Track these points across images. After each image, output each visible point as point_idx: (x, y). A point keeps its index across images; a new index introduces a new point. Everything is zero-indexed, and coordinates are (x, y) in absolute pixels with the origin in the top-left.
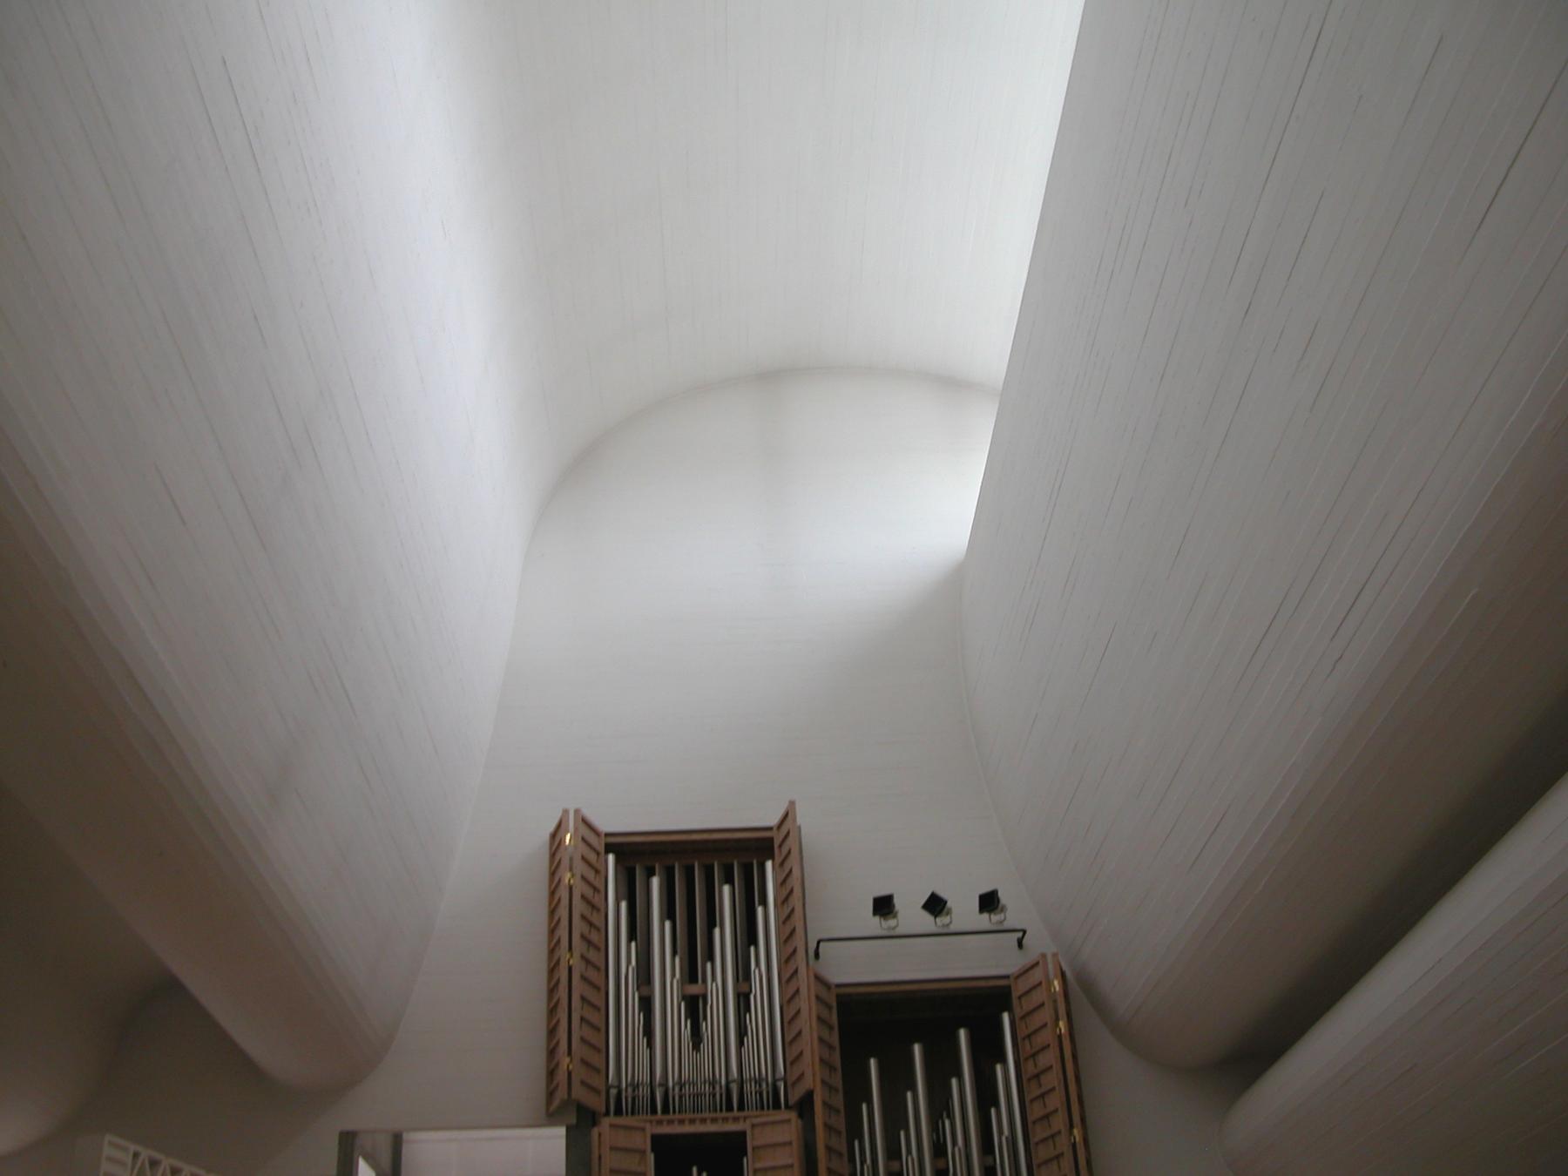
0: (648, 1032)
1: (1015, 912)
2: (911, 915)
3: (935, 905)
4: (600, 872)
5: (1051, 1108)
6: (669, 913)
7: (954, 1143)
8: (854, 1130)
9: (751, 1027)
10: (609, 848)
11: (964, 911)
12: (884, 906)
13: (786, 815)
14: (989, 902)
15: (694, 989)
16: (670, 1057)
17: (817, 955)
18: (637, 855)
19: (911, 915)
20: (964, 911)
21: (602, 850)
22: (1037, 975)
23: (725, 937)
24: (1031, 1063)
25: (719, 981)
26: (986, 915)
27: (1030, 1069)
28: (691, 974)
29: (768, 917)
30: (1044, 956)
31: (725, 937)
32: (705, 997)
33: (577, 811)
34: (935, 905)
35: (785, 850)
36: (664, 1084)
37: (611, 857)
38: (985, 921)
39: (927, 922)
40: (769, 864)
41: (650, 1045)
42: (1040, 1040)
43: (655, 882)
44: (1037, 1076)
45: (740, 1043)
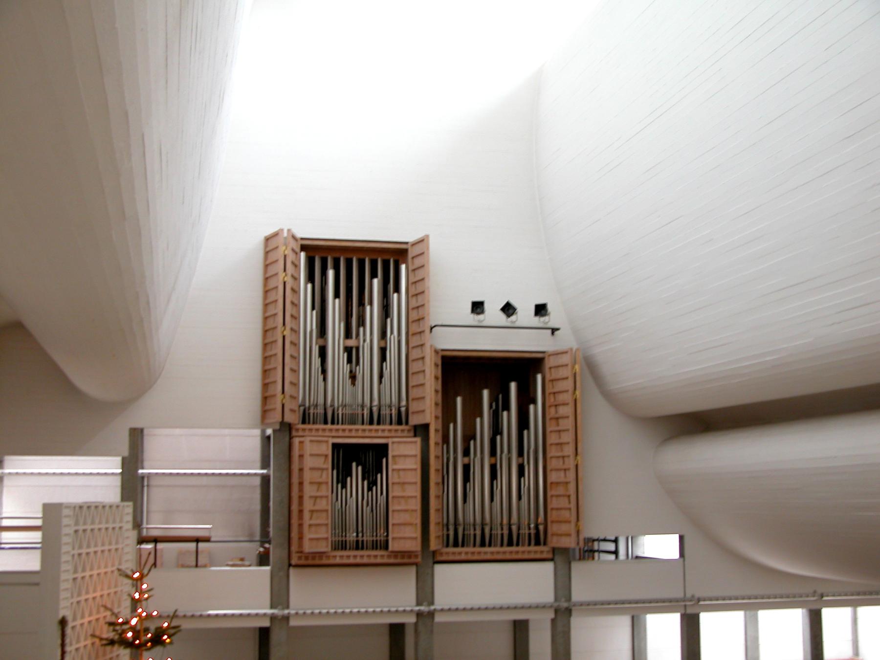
0: (324, 372)
1: (553, 318)
2: (493, 313)
3: (508, 309)
4: (296, 266)
5: (562, 441)
6: (337, 295)
7: (502, 452)
8: (445, 439)
9: (386, 373)
10: (303, 248)
11: (525, 314)
12: (478, 307)
13: (421, 241)
14: (541, 310)
15: (351, 343)
16: (337, 389)
17: (432, 328)
18: (320, 256)
19: (493, 313)
20: (525, 314)
21: (298, 249)
22: (565, 359)
23: (373, 312)
24: (553, 410)
25: (369, 339)
26: (537, 318)
27: (551, 412)
28: (348, 335)
29: (399, 301)
30: (571, 349)
31: (373, 312)
32: (358, 349)
33: (289, 230)
34: (508, 309)
35: (418, 262)
36: (332, 405)
37: (303, 254)
38: (537, 321)
39: (501, 319)
40: (403, 267)
41: (325, 379)
42: (561, 398)
43: (331, 273)
44: (557, 419)
45: (380, 382)
